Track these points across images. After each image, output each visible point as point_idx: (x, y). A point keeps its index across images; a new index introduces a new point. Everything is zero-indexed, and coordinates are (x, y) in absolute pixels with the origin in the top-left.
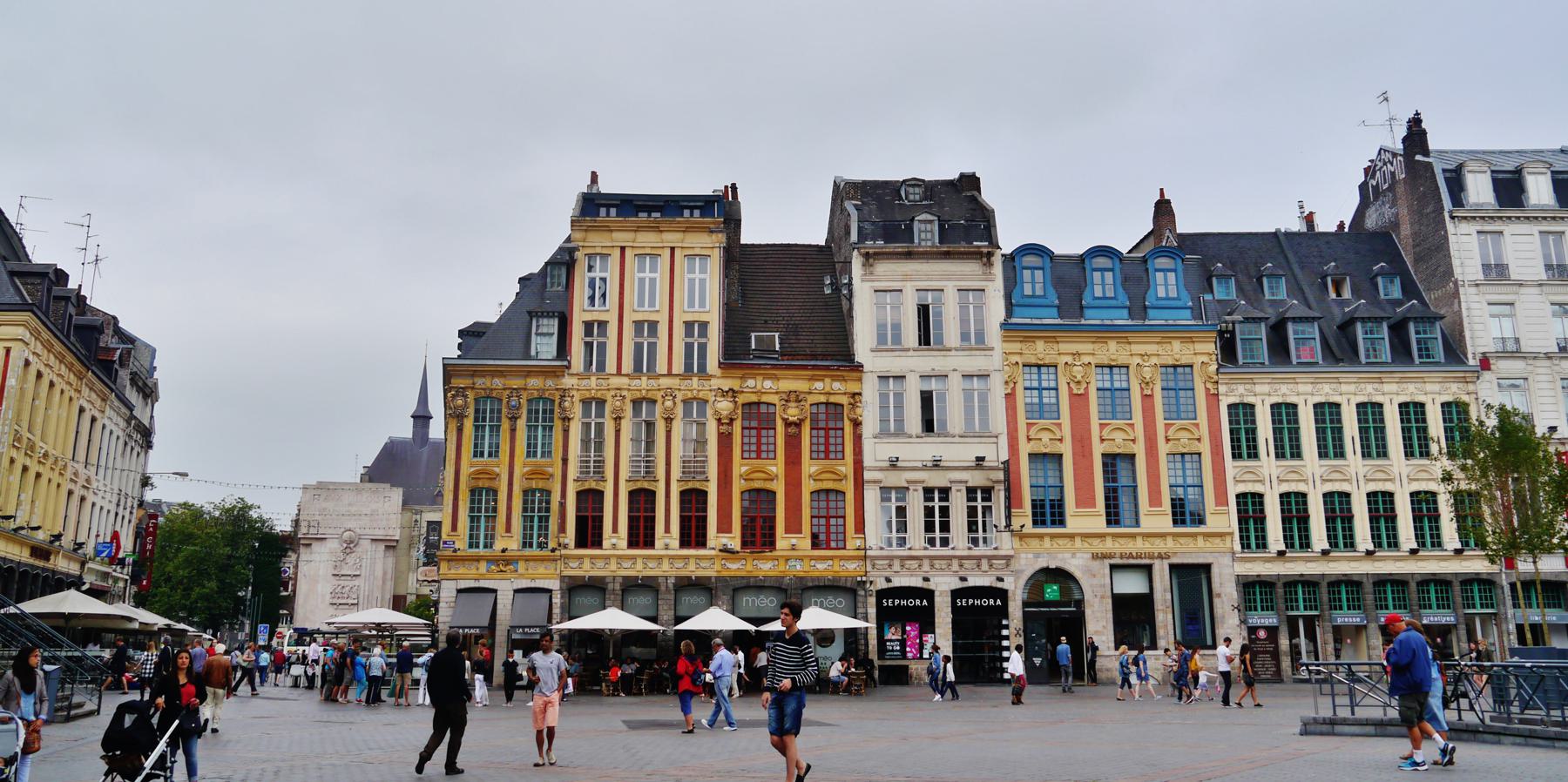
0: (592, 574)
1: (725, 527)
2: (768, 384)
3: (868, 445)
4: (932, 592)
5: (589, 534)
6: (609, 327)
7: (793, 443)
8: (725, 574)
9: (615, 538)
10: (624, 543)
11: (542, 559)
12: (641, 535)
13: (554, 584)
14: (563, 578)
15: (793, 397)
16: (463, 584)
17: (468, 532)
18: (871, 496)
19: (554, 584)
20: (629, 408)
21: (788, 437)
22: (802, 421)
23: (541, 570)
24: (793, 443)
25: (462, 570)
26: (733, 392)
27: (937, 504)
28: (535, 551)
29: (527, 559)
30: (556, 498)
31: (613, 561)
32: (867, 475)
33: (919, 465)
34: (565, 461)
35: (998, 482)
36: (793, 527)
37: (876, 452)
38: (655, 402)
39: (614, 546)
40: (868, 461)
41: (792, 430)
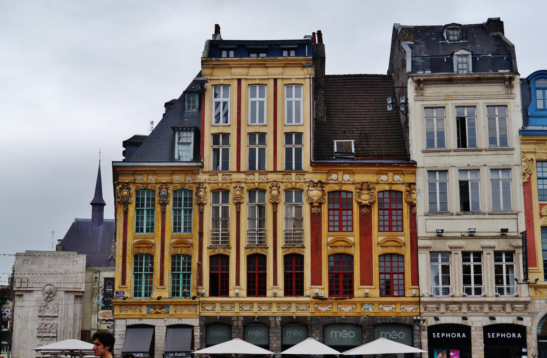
0: (300, 314)
1: (316, 281)
2: (347, 177)
3: (421, 221)
4: (525, 328)
5: (219, 286)
6: (267, 137)
7: (365, 220)
8: (317, 314)
9: (238, 289)
10: (244, 293)
11: (186, 304)
12: (257, 286)
13: (195, 322)
14: (201, 318)
15: (365, 186)
16: (131, 322)
17: (133, 285)
18: (423, 258)
19: (195, 322)
20: (283, 197)
21: (361, 215)
22: (372, 204)
23: (186, 312)
24: (365, 220)
25: (129, 312)
26: (321, 184)
27: (504, 264)
28: (181, 299)
29: (176, 304)
30: (195, 260)
31: (237, 305)
32: (420, 243)
33: (459, 235)
34: (201, 234)
35: (518, 247)
36: (367, 280)
37: (426, 226)
38: (264, 191)
39: (237, 295)
40: (421, 232)
41: (365, 210)
